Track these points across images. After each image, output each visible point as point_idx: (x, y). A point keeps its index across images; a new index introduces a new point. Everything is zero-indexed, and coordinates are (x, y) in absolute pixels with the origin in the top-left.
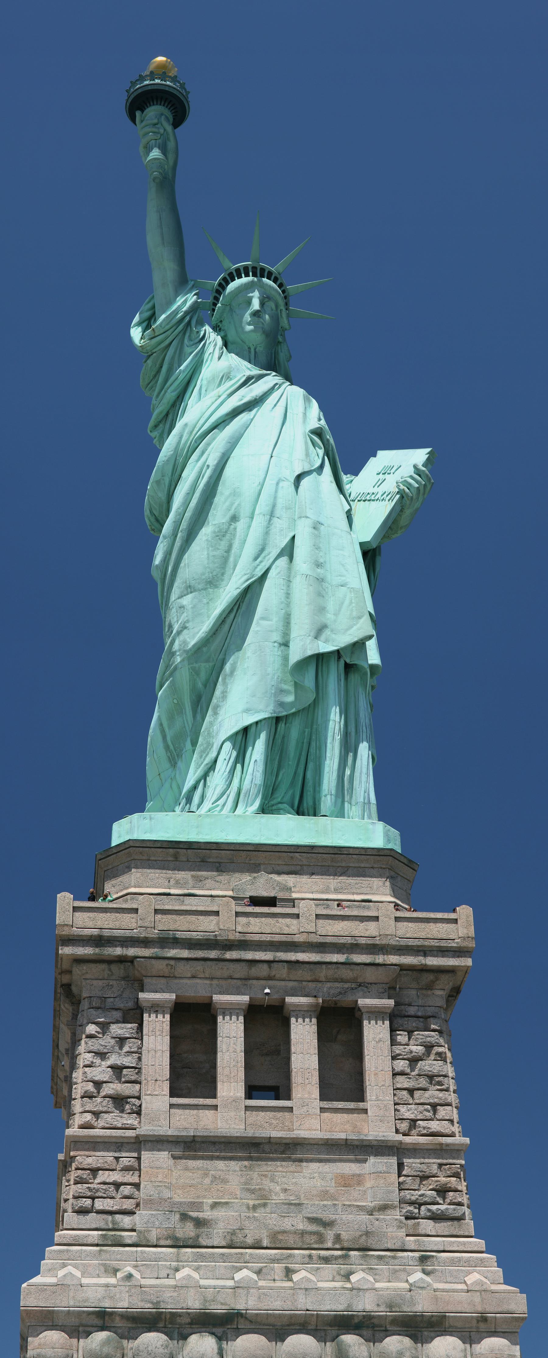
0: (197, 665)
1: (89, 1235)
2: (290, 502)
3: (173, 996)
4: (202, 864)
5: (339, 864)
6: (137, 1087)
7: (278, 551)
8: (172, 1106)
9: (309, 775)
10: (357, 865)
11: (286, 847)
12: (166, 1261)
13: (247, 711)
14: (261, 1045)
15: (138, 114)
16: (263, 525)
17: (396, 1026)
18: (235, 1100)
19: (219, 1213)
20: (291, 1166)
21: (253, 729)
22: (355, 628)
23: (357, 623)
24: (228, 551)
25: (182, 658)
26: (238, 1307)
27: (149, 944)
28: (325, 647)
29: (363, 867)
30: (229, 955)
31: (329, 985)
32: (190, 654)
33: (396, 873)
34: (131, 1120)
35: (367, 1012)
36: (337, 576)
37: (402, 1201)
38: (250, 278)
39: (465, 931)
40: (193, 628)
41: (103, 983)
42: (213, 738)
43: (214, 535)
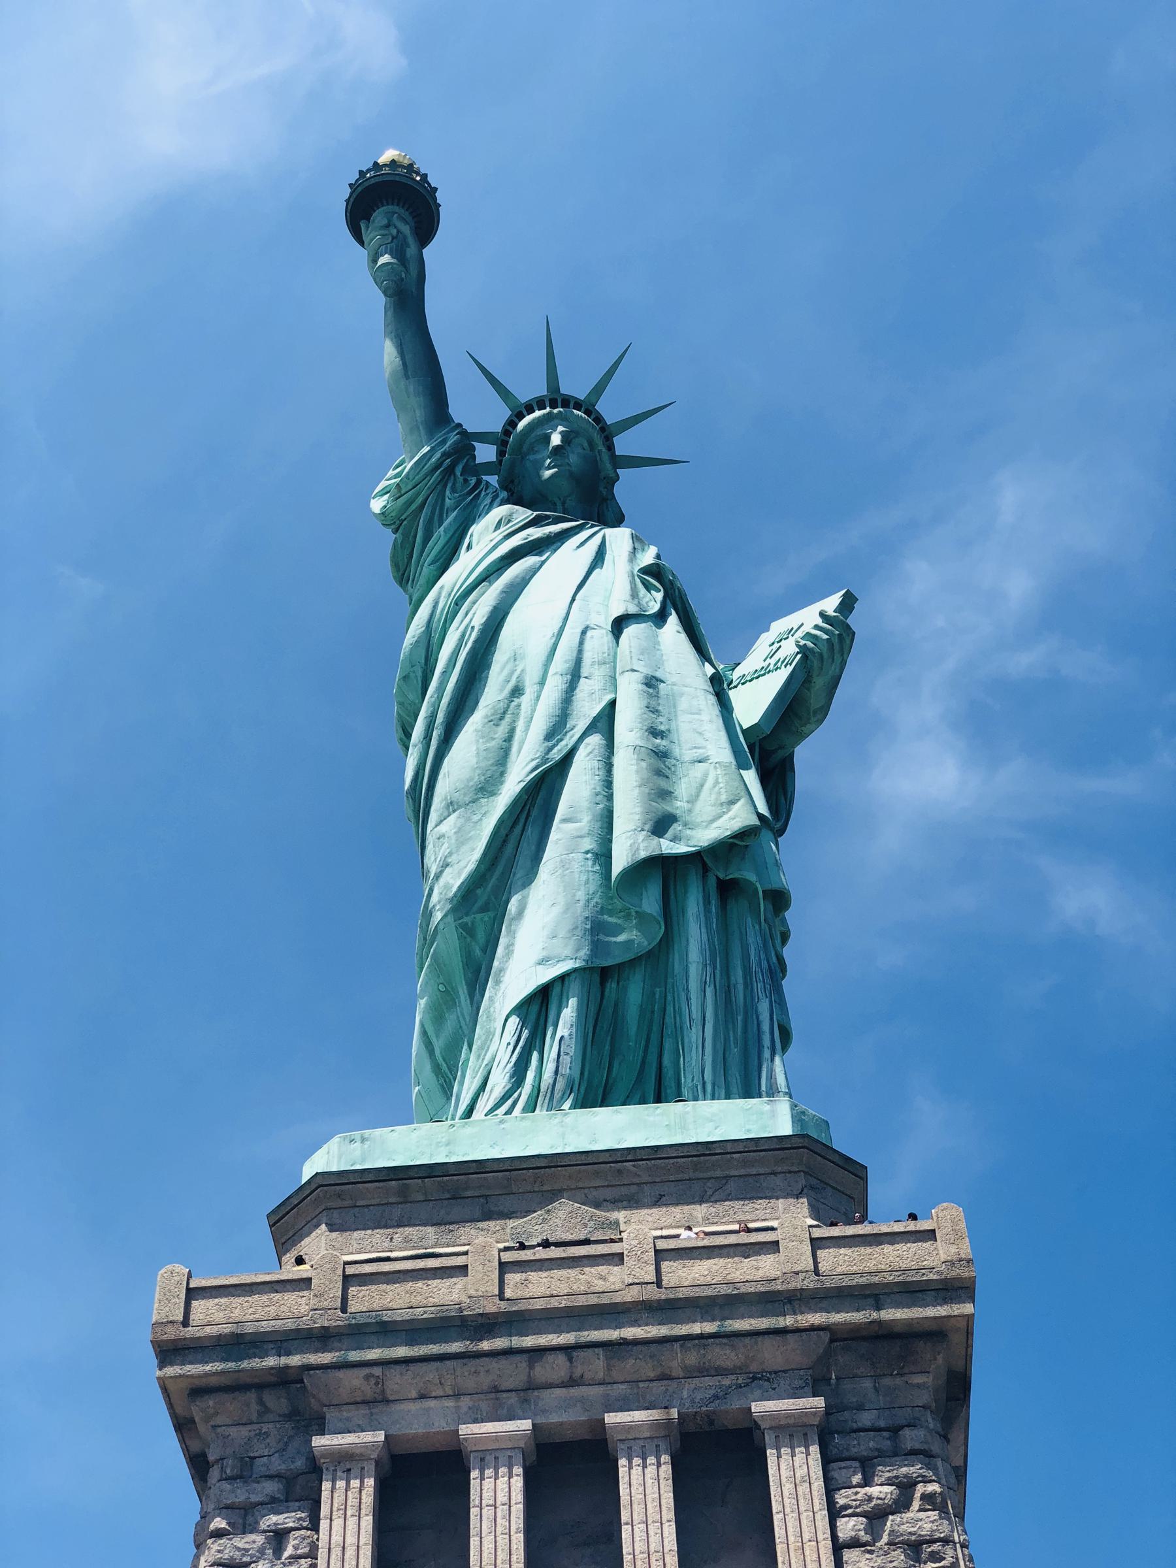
0: (465, 919)
2: (606, 655)
3: (380, 1436)
4: (453, 1202)
5: (709, 1174)
7: (588, 722)
10: (742, 1172)
11: (607, 1154)
13: (543, 961)
14: (572, 1526)
15: (363, 225)
16: (560, 688)
17: (835, 1451)
21: (556, 991)
22: (726, 817)
23: (729, 810)
24: (509, 739)
25: (444, 913)
27: (332, 1339)
29: (755, 1175)
30: (485, 1345)
32: (455, 902)
33: (821, 1181)
35: (770, 1428)
36: (691, 750)
39: (953, 1249)
40: (458, 862)
41: (250, 1431)
42: (495, 1022)
43: (486, 720)
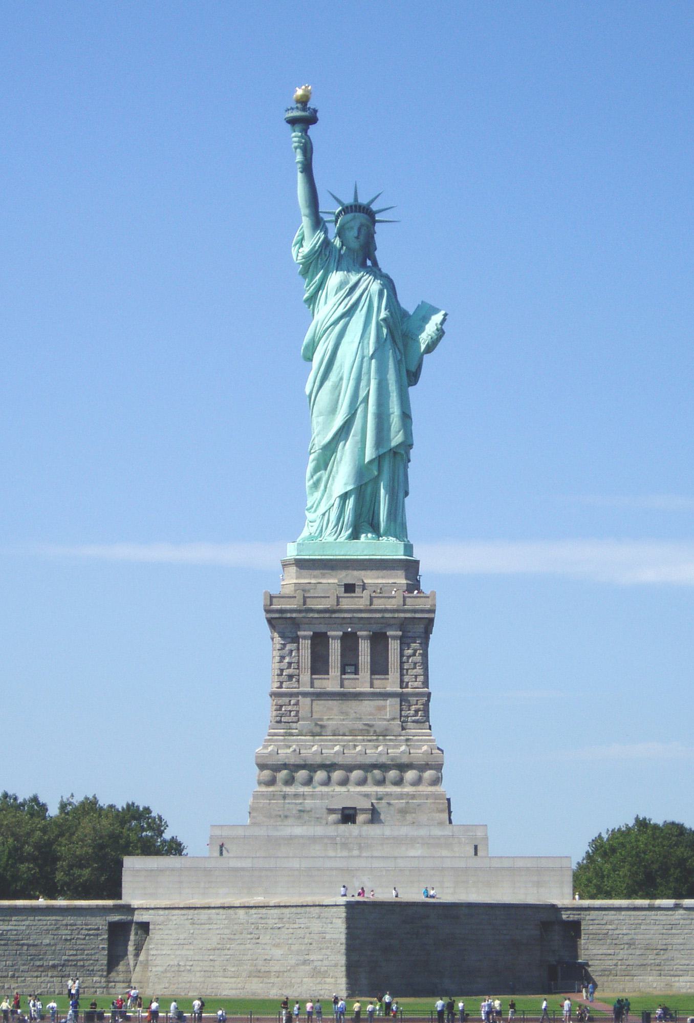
1: (280, 732)
6: (298, 671)
8: (312, 680)
9: (376, 509)
12: (309, 742)
13: (345, 484)
18: (336, 676)
19: (330, 722)
20: (358, 703)
21: (349, 493)
28: (382, 451)
30: (333, 616)
31: (375, 625)
34: (296, 685)
37: (401, 716)
38: (352, 214)
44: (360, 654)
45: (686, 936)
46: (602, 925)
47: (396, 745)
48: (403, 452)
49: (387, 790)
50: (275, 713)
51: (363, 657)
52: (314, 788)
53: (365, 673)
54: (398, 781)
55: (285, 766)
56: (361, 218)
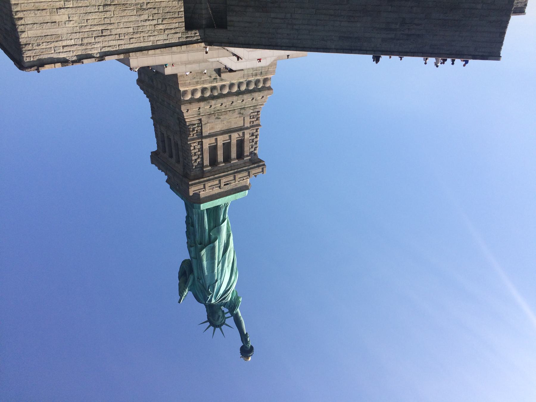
12: (247, 104)
13: (224, 225)
18: (233, 140)
19: (236, 116)
26: (237, 97)
28: (211, 245)
31: (216, 170)
37: (201, 126)
44: (222, 154)
45: (86, 24)
46: (168, 29)
47: (205, 111)
48: (199, 246)
49: (210, 85)
50: (260, 116)
51: (221, 153)
52: (246, 80)
53: (220, 144)
54: (205, 90)
55: (260, 90)
56: (218, 323)
